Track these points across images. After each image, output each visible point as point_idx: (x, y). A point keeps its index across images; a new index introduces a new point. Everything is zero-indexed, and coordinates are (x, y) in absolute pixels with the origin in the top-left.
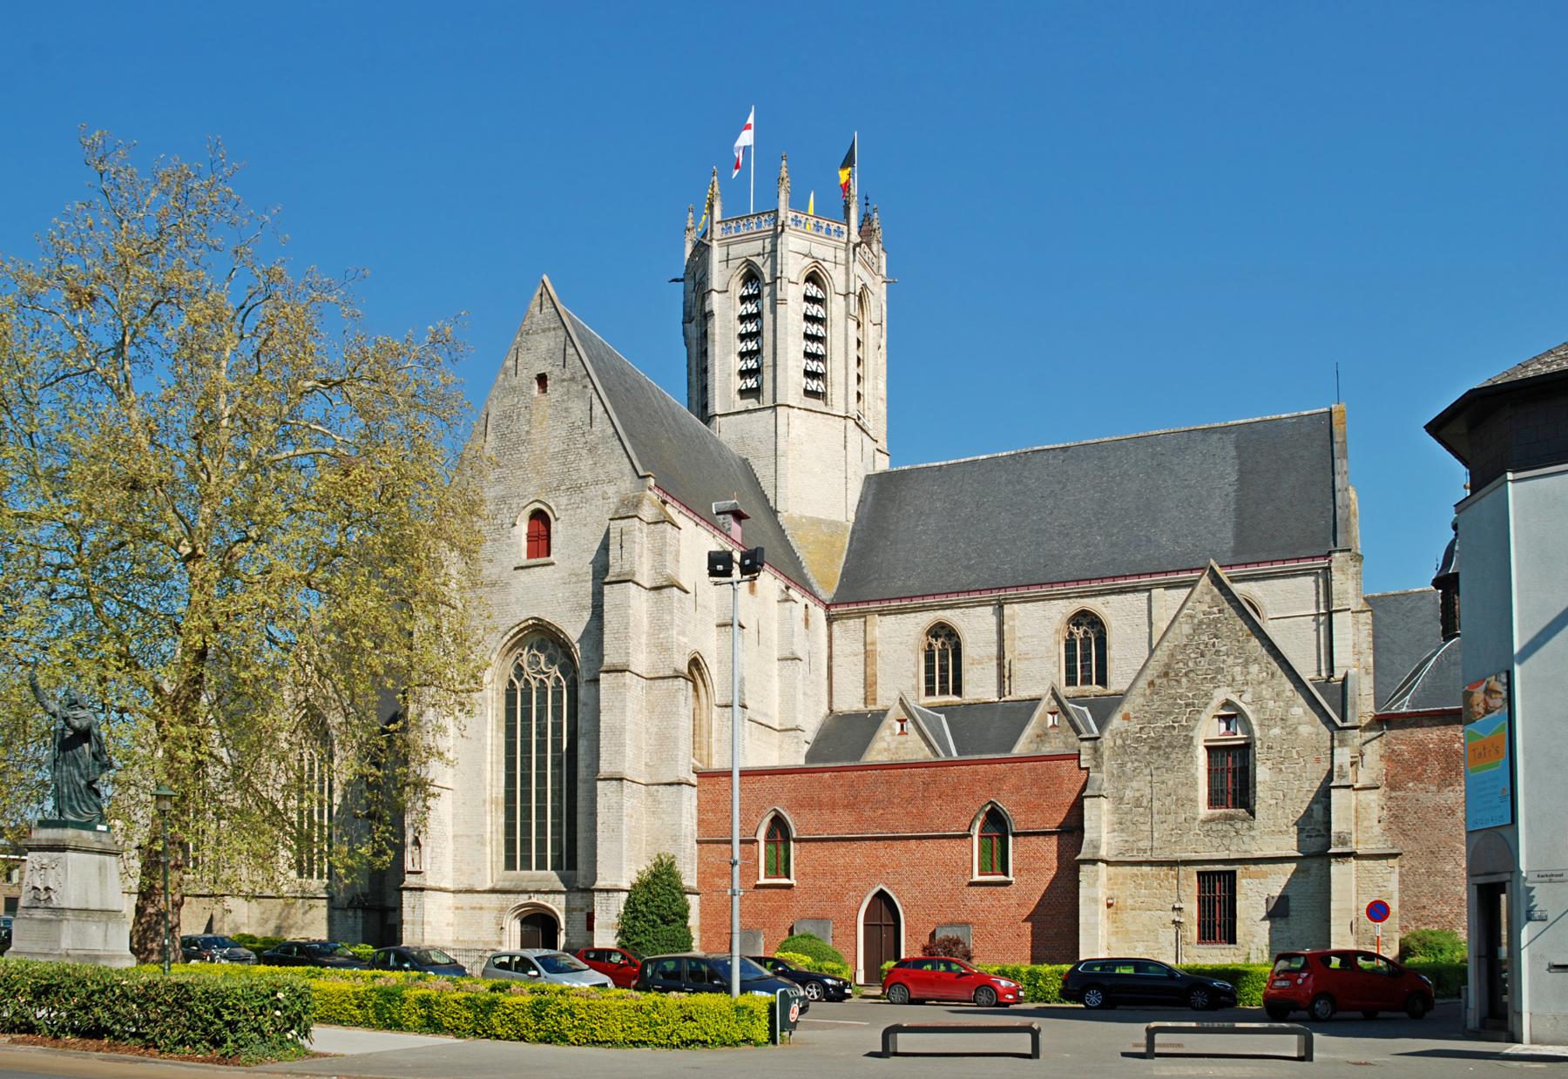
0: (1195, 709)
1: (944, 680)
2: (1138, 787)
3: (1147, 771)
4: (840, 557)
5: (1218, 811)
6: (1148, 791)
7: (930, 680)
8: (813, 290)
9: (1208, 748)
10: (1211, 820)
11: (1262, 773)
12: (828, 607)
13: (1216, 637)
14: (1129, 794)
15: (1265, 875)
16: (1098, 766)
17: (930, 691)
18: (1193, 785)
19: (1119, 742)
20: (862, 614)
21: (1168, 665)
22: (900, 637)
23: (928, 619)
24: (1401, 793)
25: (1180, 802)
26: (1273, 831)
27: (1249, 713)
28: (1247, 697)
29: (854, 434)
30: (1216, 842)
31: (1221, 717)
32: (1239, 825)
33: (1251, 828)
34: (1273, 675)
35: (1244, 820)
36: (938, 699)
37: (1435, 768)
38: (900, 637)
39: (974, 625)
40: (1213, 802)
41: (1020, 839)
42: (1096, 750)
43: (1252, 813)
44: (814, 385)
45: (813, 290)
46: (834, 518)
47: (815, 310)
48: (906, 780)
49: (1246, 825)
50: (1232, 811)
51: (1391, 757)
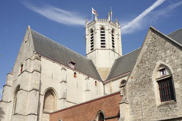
0: (151, 70)
2: (137, 98)
3: (139, 93)
4: (108, 73)
5: (163, 103)
6: (140, 99)
8: (102, 31)
9: (158, 82)
10: (161, 106)
11: (176, 85)
12: (103, 82)
13: (155, 46)
14: (134, 101)
16: (125, 94)
18: (153, 94)
19: (130, 86)
20: (109, 82)
21: (142, 59)
23: (121, 80)
27: (170, 67)
31: (160, 71)
32: (171, 106)
33: (175, 106)
35: (172, 104)
42: (124, 89)
43: (176, 101)
45: (102, 31)
46: (108, 67)
48: (83, 108)
49: (173, 106)
50: (168, 102)
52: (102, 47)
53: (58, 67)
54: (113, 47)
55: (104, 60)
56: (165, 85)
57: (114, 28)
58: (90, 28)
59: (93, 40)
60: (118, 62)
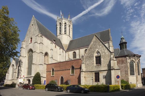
1: (75, 57)
2: (88, 62)
7: (74, 57)
8: (65, 25)
11: (102, 59)
14: (87, 63)
15: (103, 73)
16: (83, 60)
17: (74, 58)
18: (94, 62)
20: (68, 51)
22: (71, 53)
23: (73, 51)
25: (92, 64)
26: (104, 66)
28: (100, 50)
29: (69, 37)
30: (97, 69)
32: (99, 66)
33: (101, 67)
34: (103, 47)
36: (74, 59)
38: (71, 53)
39: (77, 51)
40: (96, 64)
41: (75, 69)
43: (101, 65)
44: (65, 33)
45: (65, 25)
47: (65, 26)
50: (98, 65)
52: (65, 33)
53: (49, 42)
54: (69, 34)
55: (66, 40)
56: (98, 58)
57: (70, 24)
58: (60, 22)
59: (60, 29)
60: (71, 42)
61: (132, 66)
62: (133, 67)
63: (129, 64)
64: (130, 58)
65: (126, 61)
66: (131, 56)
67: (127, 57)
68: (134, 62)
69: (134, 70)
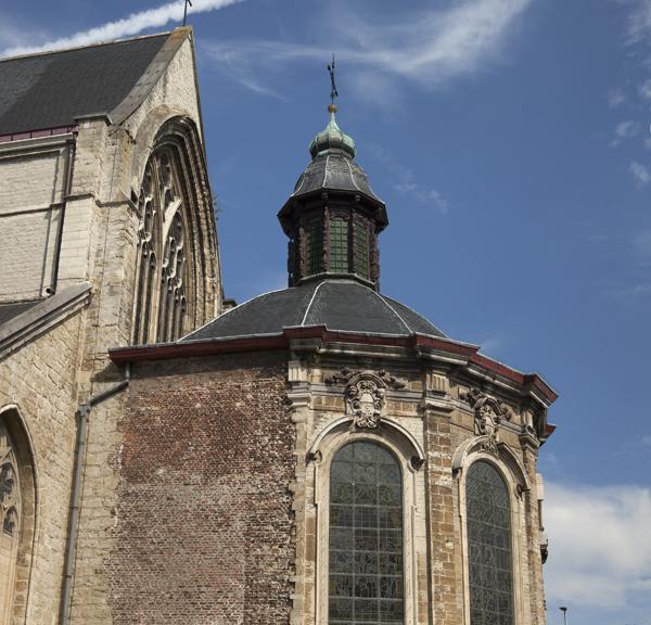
24: (144, 487)
37: (201, 443)
51: (134, 426)
61: (368, 517)
62: (396, 541)
63: (315, 491)
64: (350, 395)
65: (286, 433)
66: (358, 362)
67: (296, 374)
68: (405, 463)
69: (398, 588)
